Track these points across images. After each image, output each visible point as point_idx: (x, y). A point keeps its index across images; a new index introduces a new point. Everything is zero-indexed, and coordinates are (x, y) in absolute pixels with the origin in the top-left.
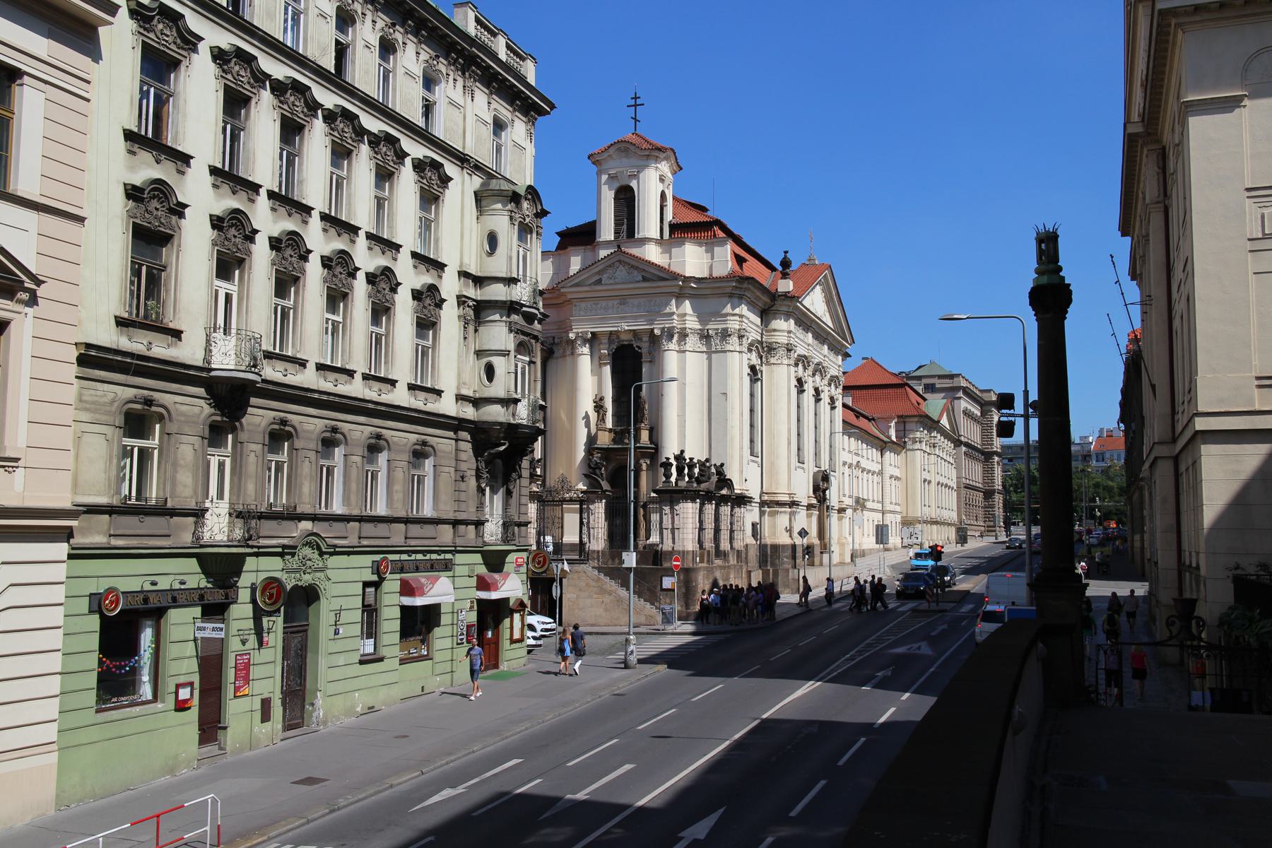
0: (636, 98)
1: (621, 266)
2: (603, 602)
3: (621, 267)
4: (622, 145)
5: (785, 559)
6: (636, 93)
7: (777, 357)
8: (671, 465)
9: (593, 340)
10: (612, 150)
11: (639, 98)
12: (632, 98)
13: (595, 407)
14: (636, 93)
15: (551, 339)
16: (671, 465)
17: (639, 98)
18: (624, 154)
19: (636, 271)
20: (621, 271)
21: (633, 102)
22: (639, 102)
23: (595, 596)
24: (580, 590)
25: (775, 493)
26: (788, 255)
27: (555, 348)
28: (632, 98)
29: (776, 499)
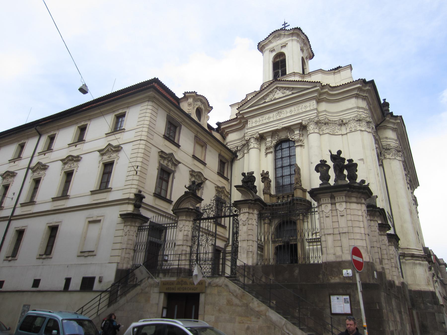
0: (285, 24)
1: (278, 90)
2: (248, 328)
3: (278, 92)
4: (277, 34)
5: (428, 304)
6: (285, 22)
7: (391, 155)
8: (329, 167)
9: (261, 138)
10: (270, 38)
11: (287, 23)
12: (283, 25)
13: (262, 179)
14: (285, 22)
15: (236, 149)
16: (329, 167)
17: (287, 23)
18: (278, 38)
19: (288, 91)
20: (278, 94)
21: (284, 26)
22: (286, 25)
23: (238, 319)
24: (220, 310)
25: (408, 249)
26: (386, 101)
27: (238, 154)
28: (283, 25)
29: (411, 253)
